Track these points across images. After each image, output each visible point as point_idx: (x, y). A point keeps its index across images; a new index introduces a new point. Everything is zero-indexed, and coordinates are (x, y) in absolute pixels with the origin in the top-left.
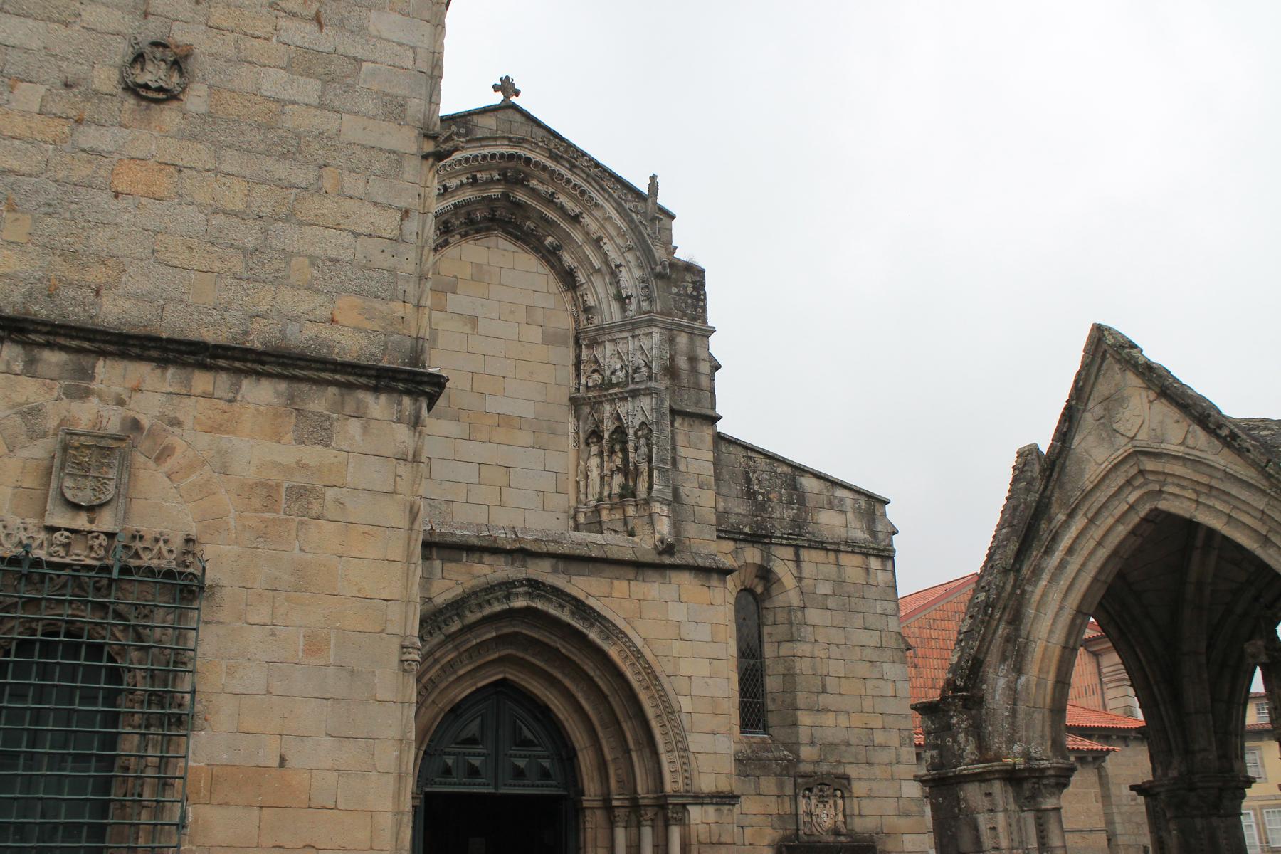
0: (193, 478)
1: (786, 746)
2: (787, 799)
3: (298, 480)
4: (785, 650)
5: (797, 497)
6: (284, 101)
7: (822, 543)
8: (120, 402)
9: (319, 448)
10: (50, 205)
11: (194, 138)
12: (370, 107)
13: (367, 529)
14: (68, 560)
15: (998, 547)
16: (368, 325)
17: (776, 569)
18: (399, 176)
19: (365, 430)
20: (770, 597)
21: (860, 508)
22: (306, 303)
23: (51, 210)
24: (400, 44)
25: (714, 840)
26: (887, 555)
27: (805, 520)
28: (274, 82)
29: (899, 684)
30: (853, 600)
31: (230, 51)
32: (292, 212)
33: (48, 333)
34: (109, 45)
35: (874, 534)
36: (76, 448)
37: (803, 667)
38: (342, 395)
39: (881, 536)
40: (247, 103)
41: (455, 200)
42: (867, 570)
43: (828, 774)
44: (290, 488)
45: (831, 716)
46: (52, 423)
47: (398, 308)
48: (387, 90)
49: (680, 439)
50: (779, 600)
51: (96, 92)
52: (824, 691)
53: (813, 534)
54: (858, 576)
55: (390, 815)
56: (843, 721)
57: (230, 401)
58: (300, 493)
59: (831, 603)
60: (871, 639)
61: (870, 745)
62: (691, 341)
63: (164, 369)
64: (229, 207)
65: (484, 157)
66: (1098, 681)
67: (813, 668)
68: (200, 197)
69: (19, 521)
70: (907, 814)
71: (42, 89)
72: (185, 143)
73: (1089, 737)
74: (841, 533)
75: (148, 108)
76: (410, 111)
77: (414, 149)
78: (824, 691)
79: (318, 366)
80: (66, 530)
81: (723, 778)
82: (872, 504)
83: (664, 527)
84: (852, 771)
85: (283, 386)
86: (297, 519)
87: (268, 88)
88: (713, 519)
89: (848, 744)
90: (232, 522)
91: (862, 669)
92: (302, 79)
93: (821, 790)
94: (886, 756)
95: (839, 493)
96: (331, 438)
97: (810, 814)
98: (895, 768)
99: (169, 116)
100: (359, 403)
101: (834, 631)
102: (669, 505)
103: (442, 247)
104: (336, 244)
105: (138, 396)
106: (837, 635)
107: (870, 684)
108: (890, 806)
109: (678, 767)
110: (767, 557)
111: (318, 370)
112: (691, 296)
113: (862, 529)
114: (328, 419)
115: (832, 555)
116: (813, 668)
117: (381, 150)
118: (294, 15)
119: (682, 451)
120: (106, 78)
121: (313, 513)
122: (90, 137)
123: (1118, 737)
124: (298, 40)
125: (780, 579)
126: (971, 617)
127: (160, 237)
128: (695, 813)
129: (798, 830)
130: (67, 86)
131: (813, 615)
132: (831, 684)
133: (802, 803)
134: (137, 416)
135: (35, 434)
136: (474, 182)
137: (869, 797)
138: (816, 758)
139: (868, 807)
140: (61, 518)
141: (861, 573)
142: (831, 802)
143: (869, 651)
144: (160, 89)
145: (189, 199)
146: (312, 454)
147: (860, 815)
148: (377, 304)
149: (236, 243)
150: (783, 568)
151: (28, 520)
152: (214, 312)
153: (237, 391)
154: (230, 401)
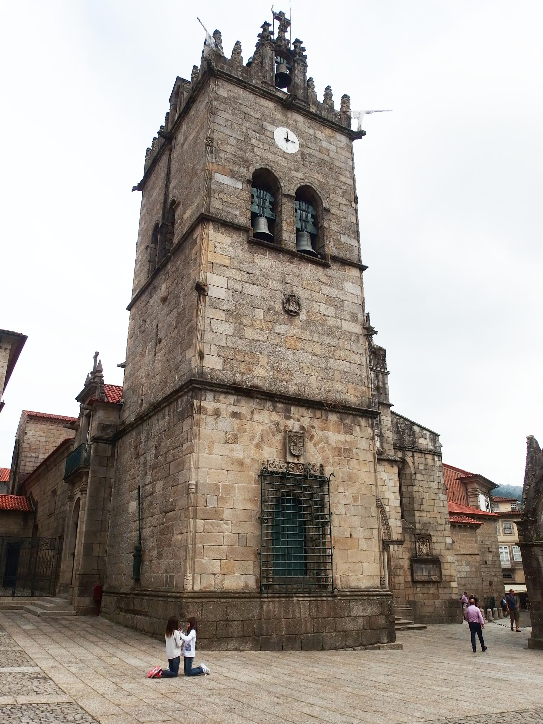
0: (320, 445)
1: (411, 523)
3: (346, 446)
4: (410, 489)
5: (413, 433)
6: (326, 315)
7: (421, 450)
8: (299, 421)
9: (350, 435)
10: (271, 353)
11: (304, 329)
12: (348, 317)
13: (364, 462)
14: (294, 473)
15: (528, 470)
16: (357, 394)
17: (407, 460)
19: (360, 429)
20: (404, 469)
21: (431, 437)
22: (340, 387)
23: (271, 354)
24: (353, 294)
25: (397, 557)
26: (439, 455)
27: (415, 441)
28: (323, 308)
29: (445, 502)
30: (430, 471)
31: (310, 297)
32: (333, 355)
33: (280, 398)
34: (278, 295)
35: (435, 447)
36: (293, 437)
37: (416, 495)
38: (354, 418)
39: (438, 448)
40: (316, 316)
42: (434, 460)
43: (424, 534)
44: (344, 449)
46: (282, 428)
47: (364, 389)
48: (352, 311)
50: (407, 471)
51: (277, 312)
52: (422, 504)
53: (417, 447)
54: (430, 462)
55: (378, 552)
56: (428, 515)
57: (326, 420)
58: (347, 450)
59: (423, 472)
60: (435, 485)
61: (437, 524)
62: (383, 376)
63: (308, 410)
64: (317, 354)
66: (465, 494)
68: (309, 350)
69: (279, 460)
70: (448, 549)
71: (263, 311)
72: (302, 331)
73: (473, 518)
74: (426, 447)
75: (291, 318)
76: (359, 319)
77: (361, 333)
78: (422, 504)
79: (349, 409)
80: (292, 463)
81: (399, 535)
82: (435, 436)
83: (378, 444)
84: (432, 533)
85: (339, 415)
86: (347, 459)
87: (322, 311)
89: (430, 523)
90: (331, 460)
91: (433, 496)
92: (330, 307)
93: (423, 540)
94: (441, 528)
95: (425, 432)
96: (352, 432)
97: (419, 548)
98: (444, 532)
99: (297, 321)
100: (359, 421)
101: (425, 482)
102: (379, 437)
104: (344, 366)
105: (303, 418)
106: (425, 484)
107: (436, 502)
108: (443, 546)
109: (386, 531)
110: (404, 455)
111: (349, 410)
112: (382, 360)
113: (432, 445)
114: (351, 426)
115: (423, 455)
117: (353, 333)
118: (324, 283)
120: (278, 307)
121: (351, 457)
122: (278, 328)
123: (478, 518)
124: (326, 293)
125: (408, 463)
126: (526, 494)
127: (301, 364)
128: (392, 547)
129: (416, 553)
130: (269, 310)
133: (417, 544)
134: (304, 425)
135: (279, 431)
137: (437, 542)
138: (420, 528)
139: (437, 546)
140: (290, 460)
141: (432, 461)
143: (435, 490)
144: (296, 312)
145: (306, 351)
146: (349, 438)
147: (434, 549)
148: (358, 387)
149: (320, 366)
150: (409, 460)
151: (281, 460)
152: (317, 390)
153: (327, 417)
154: (326, 420)
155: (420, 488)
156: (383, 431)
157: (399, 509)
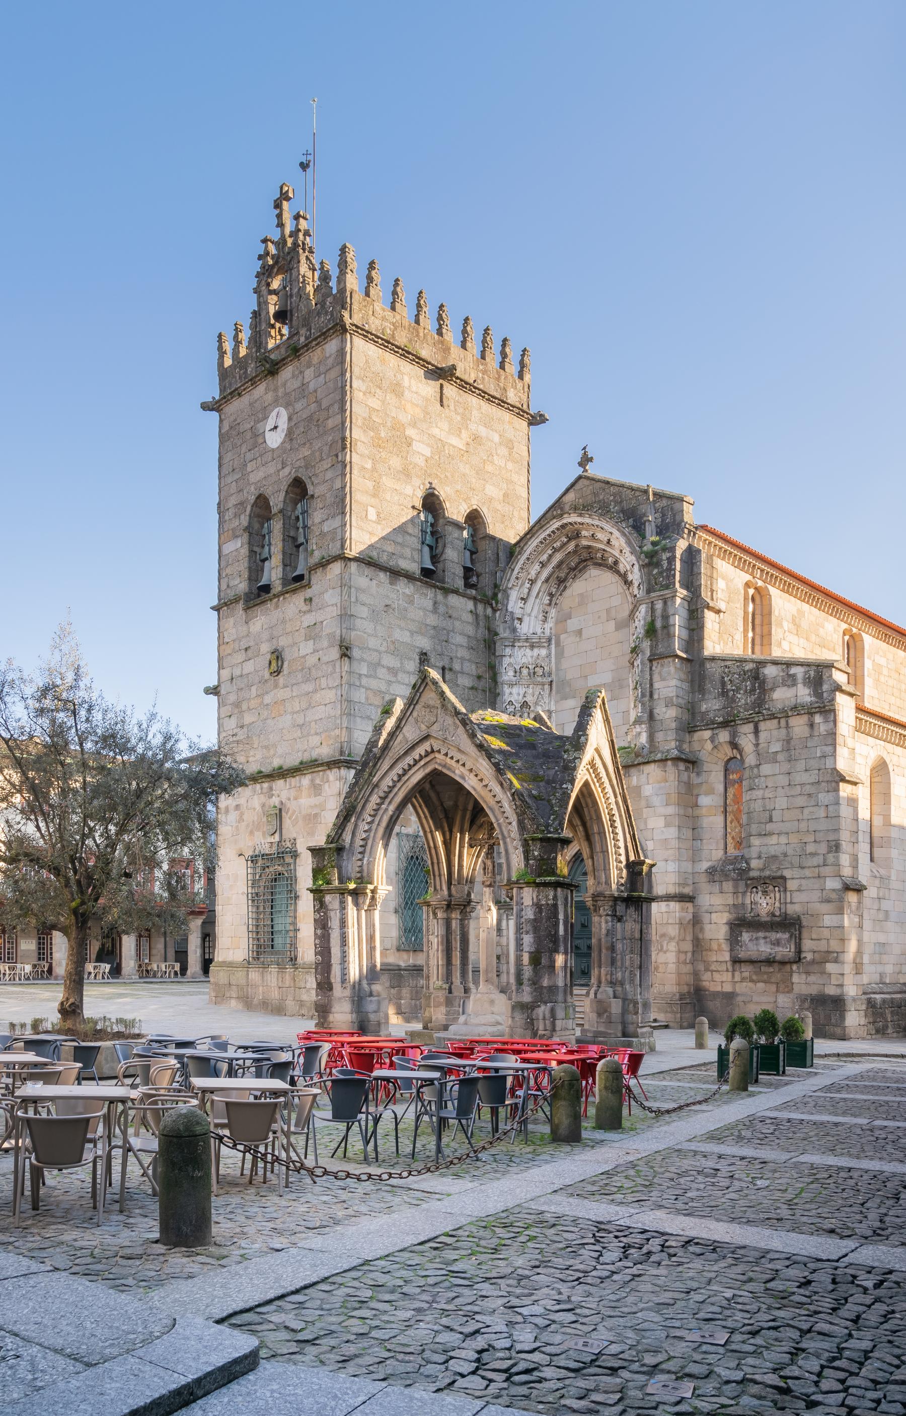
2: (740, 895)
12: (325, 643)
18: (335, 672)
41: (553, 565)
45: (775, 837)
47: (337, 732)
49: (656, 677)
52: (771, 820)
56: (783, 840)
61: (803, 854)
65: (549, 535)
67: (764, 806)
70: (828, 901)
78: (771, 820)
84: (787, 873)
88: (674, 725)
89: (785, 855)
98: (821, 869)
103: (563, 590)
110: (734, 735)
116: (764, 806)
119: (656, 685)
131: (766, 769)
132: (776, 816)
136: (556, 550)
139: (798, 897)
141: (807, 729)
142: (772, 895)
147: (791, 903)
155: (767, 791)
156: (656, 711)
157: (674, 843)
